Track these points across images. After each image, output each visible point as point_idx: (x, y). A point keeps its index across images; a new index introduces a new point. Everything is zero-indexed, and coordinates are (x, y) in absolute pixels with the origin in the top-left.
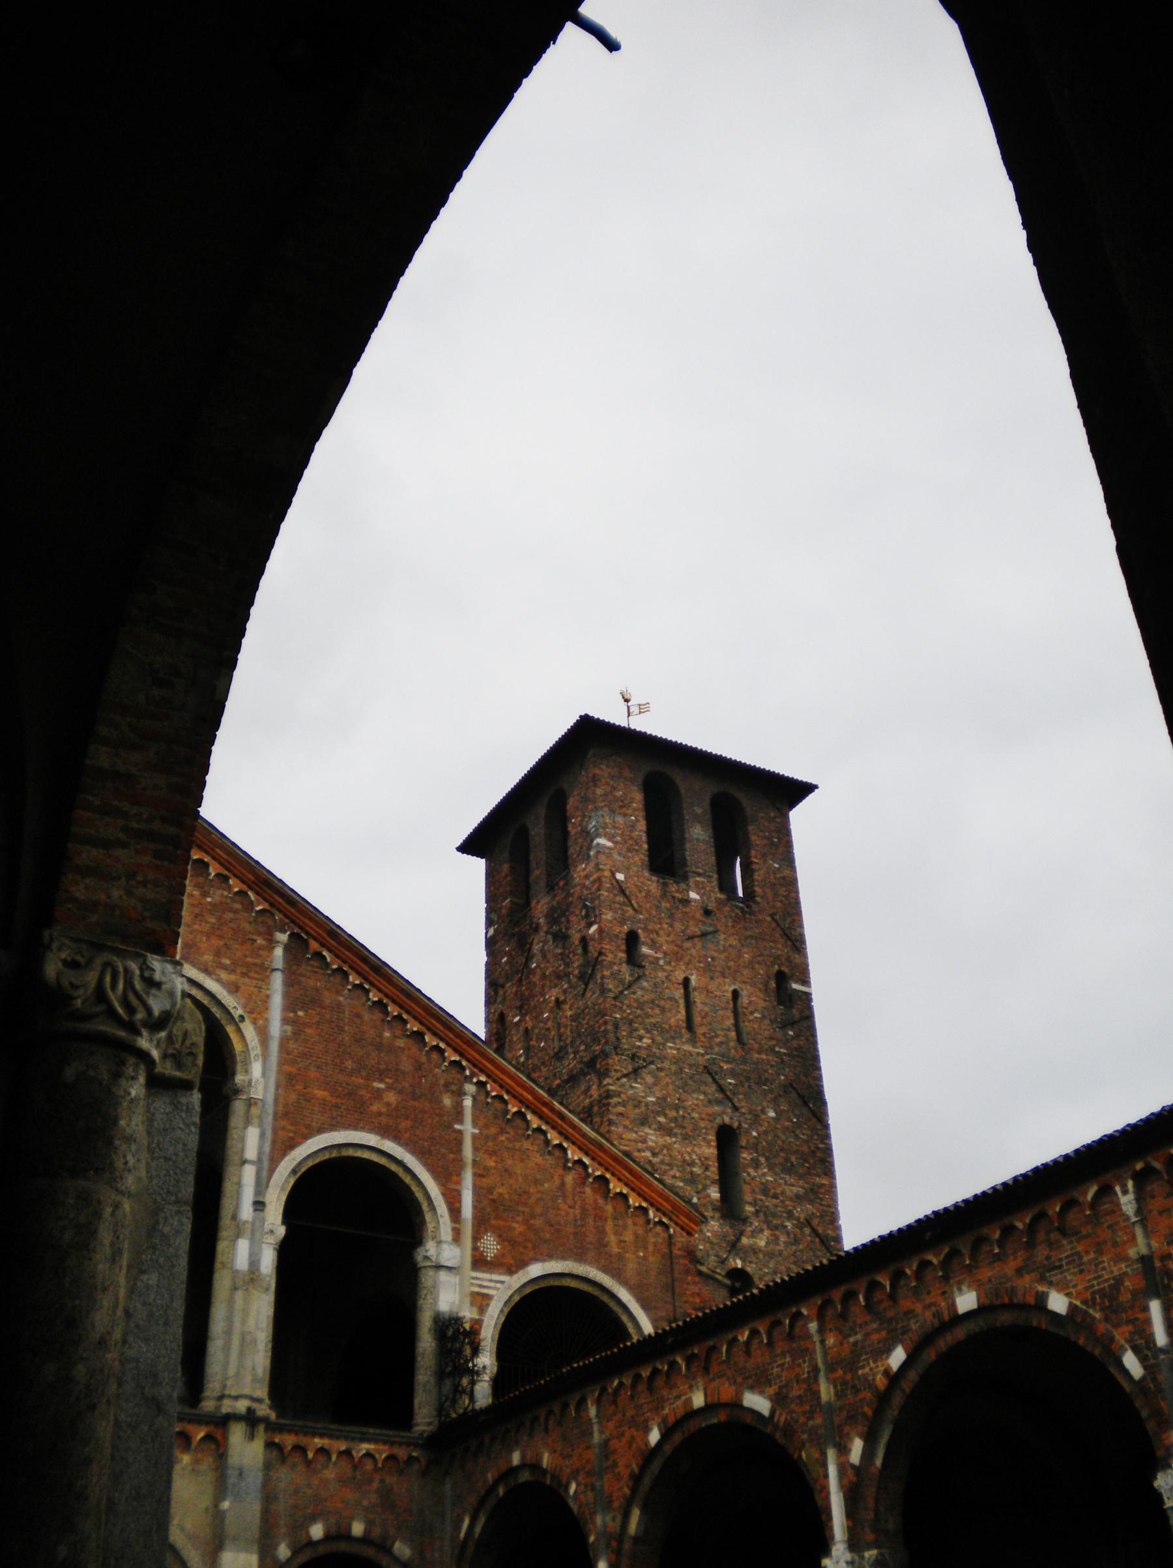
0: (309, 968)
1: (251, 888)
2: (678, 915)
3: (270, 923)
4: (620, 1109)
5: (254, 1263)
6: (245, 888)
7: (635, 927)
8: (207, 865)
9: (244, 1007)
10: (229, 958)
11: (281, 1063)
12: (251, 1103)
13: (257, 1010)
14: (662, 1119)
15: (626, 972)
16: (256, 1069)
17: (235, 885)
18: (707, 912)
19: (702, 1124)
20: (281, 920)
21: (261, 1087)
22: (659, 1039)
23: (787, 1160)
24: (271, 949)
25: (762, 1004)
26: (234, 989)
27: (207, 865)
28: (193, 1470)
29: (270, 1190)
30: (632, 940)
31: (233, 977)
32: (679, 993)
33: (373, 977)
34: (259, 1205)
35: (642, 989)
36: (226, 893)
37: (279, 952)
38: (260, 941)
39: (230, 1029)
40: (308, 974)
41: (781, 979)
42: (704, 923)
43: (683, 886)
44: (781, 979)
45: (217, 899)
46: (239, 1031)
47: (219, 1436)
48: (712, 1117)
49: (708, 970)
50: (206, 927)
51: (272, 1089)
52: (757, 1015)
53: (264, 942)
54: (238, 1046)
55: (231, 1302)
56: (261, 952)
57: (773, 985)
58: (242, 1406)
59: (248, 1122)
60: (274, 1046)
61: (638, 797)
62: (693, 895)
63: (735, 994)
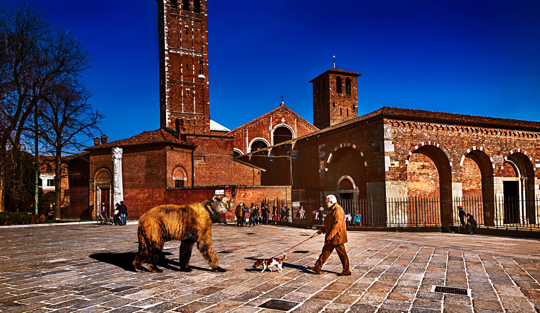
13: (294, 128)
18: (344, 97)
26: (291, 126)
30: (334, 103)
37: (296, 121)
49: (344, 106)
62: (342, 95)
63: (347, 109)
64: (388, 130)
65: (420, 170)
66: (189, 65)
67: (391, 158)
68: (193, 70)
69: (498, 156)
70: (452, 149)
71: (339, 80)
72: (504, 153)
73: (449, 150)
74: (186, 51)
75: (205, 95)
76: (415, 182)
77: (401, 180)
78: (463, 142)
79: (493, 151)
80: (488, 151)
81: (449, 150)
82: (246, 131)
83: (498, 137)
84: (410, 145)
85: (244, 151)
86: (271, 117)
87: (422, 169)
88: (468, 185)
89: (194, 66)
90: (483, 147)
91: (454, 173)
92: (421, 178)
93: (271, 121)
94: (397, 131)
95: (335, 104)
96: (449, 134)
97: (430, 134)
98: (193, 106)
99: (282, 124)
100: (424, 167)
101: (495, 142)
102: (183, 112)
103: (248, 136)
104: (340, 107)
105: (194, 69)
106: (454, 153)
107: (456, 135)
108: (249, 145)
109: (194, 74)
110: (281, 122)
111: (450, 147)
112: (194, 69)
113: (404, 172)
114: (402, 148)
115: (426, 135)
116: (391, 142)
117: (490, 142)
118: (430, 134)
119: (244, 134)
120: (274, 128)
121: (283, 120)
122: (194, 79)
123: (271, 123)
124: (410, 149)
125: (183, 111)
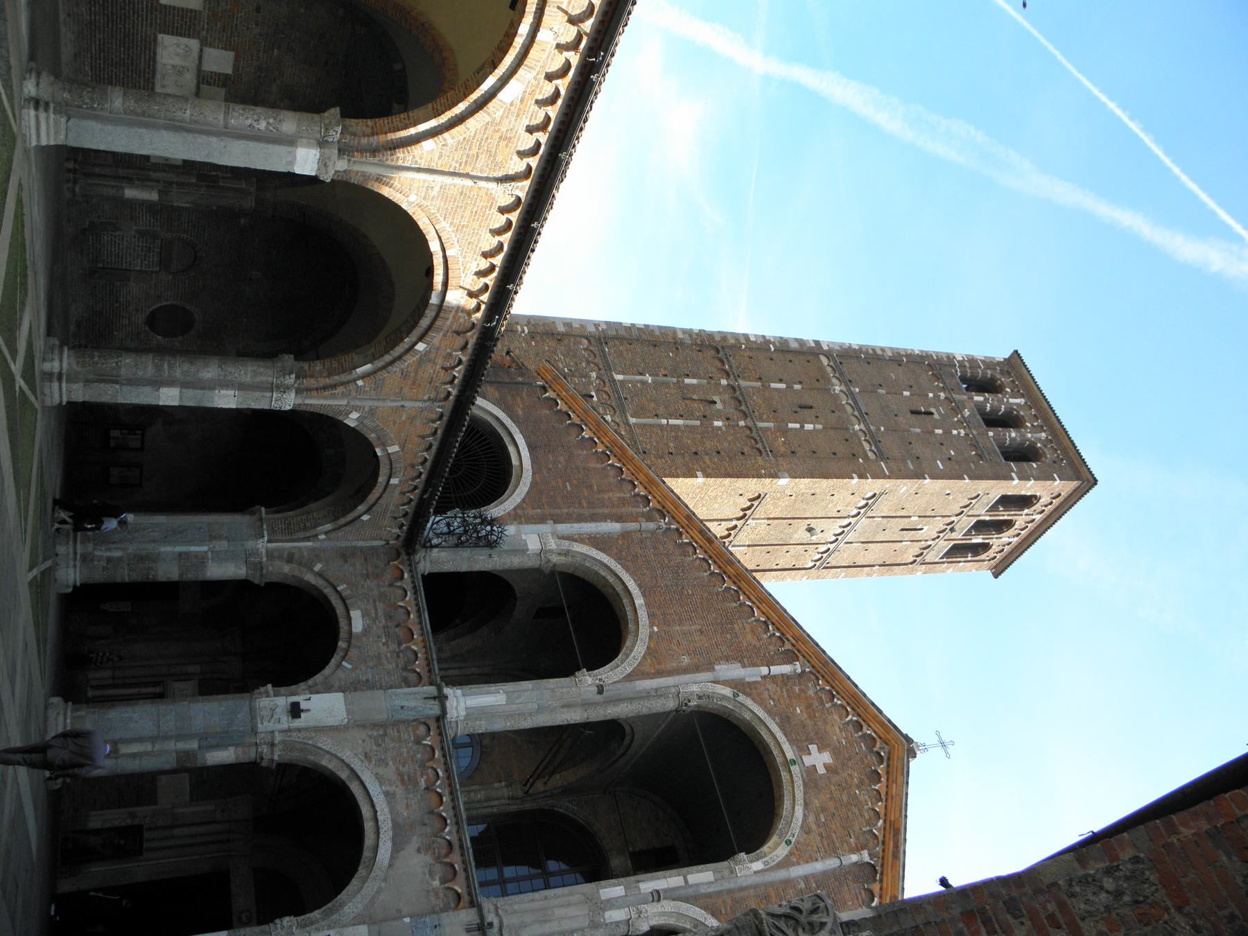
0: (857, 891)
1: (885, 821)
3: (871, 845)
5: (611, 904)
6: (882, 815)
8: (879, 781)
9: (798, 842)
10: (826, 820)
11: (772, 884)
12: (732, 871)
13: (799, 854)
16: (758, 866)
17: (879, 808)
20: (878, 853)
21: (743, 872)
26: (806, 829)
27: (879, 781)
28: (428, 891)
29: (672, 903)
31: (814, 827)
34: (657, 896)
36: (870, 804)
37: (854, 858)
39: (774, 839)
40: (853, 892)
45: (862, 798)
46: (777, 845)
47: (461, 904)
50: (837, 795)
51: (750, 881)
53: (854, 845)
54: (765, 848)
55: (571, 894)
56: (845, 844)
58: (491, 917)
59: (715, 871)
60: (781, 874)
68: (802, 427)
74: (855, 402)
82: (649, 518)
85: (531, 512)
89: (819, 427)
93: (777, 670)
98: (657, 415)
99: (790, 754)
102: (619, 377)
103: (625, 535)
105: (809, 427)
108: (570, 538)
109: (791, 425)
112: (809, 427)
119: (630, 509)
120: (741, 698)
121: (819, 759)
122: (771, 425)
123: (764, 670)
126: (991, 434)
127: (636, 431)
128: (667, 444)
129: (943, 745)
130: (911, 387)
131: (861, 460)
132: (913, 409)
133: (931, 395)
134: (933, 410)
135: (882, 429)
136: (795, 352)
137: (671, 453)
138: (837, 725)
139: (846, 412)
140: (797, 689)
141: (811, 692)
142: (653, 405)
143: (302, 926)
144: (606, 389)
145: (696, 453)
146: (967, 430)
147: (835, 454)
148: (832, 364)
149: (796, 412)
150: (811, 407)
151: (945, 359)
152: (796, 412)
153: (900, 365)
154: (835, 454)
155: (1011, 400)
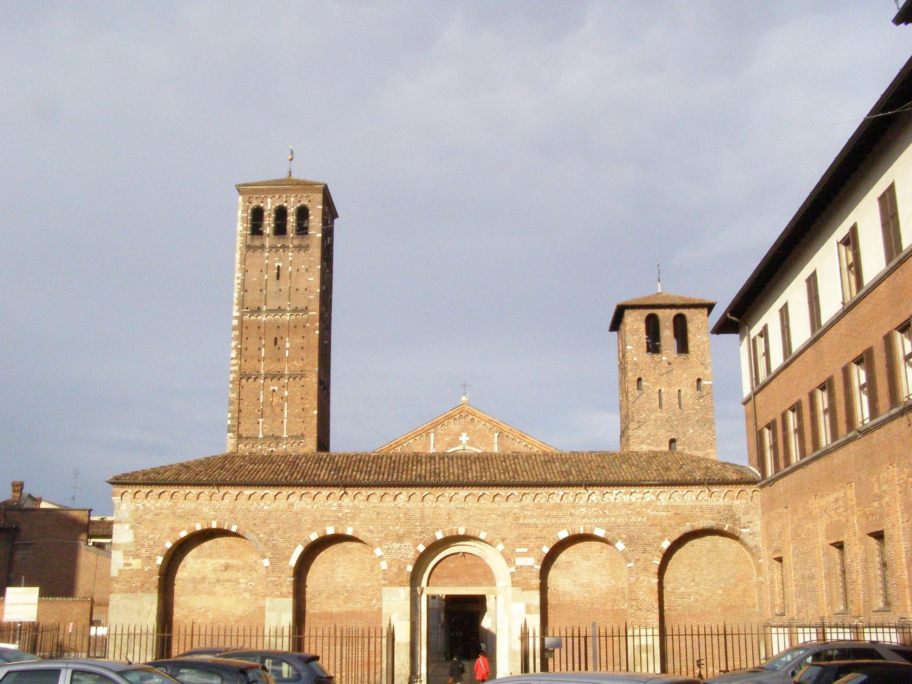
2: (657, 368)
4: (633, 440)
7: (640, 376)
14: (649, 441)
15: (637, 393)
17: (483, 423)
18: (669, 364)
19: (663, 440)
22: (648, 414)
23: (696, 446)
24: (494, 438)
25: (690, 392)
30: (639, 380)
32: (657, 396)
33: (524, 439)
35: (643, 398)
38: (491, 436)
41: (699, 380)
42: (667, 368)
43: (660, 355)
44: (699, 380)
48: (669, 436)
49: (670, 386)
50: (477, 436)
52: (688, 397)
57: (696, 384)
61: (643, 326)
64: (124, 506)
65: (218, 573)
66: (279, 339)
67: (126, 554)
68: (288, 349)
69: (396, 545)
70: (271, 533)
71: (653, 327)
72: (414, 537)
73: (261, 535)
75: (309, 396)
76: (205, 596)
77: (143, 592)
78: (299, 520)
79: (383, 535)
80: (368, 534)
81: (261, 535)
83: (399, 506)
84: (168, 530)
86: (432, 435)
87: (222, 571)
88: (341, 602)
89: (287, 339)
90: (355, 527)
91: (273, 579)
92: (218, 588)
93: (432, 443)
94: (142, 507)
95: (644, 383)
96: (266, 505)
97: (217, 507)
98: (282, 422)
99: (461, 448)
100: (227, 567)
101: (389, 517)
102: (261, 436)
104: (658, 391)
106: (275, 542)
107: (281, 507)
109: (287, 355)
110: (460, 443)
111: (266, 530)
112: (288, 345)
113: (152, 577)
114: (151, 536)
115: (205, 510)
116: (127, 526)
117: (374, 516)
118: (217, 507)
121: (464, 438)
122: (287, 365)
124: (169, 537)
125: (261, 434)
126: (291, 235)
127: (291, 434)
128: (298, 422)
129: (464, 386)
130: (261, 271)
131: (308, 325)
132: (276, 277)
133: (267, 261)
134: (277, 265)
135: (289, 303)
136: (241, 333)
137: (303, 422)
138: (454, 426)
139: (278, 320)
140: (440, 437)
141: (442, 432)
142: (276, 422)
143: (489, 600)
144: (269, 443)
145: (303, 409)
146: (290, 250)
147: (303, 337)
148: (249, 315)
149: (279, 348)
150: (276, 339)
151: (242, 238)
152: (279, 348)
153: (247, 271)
154: (303, 337)
155: (269, 208)
